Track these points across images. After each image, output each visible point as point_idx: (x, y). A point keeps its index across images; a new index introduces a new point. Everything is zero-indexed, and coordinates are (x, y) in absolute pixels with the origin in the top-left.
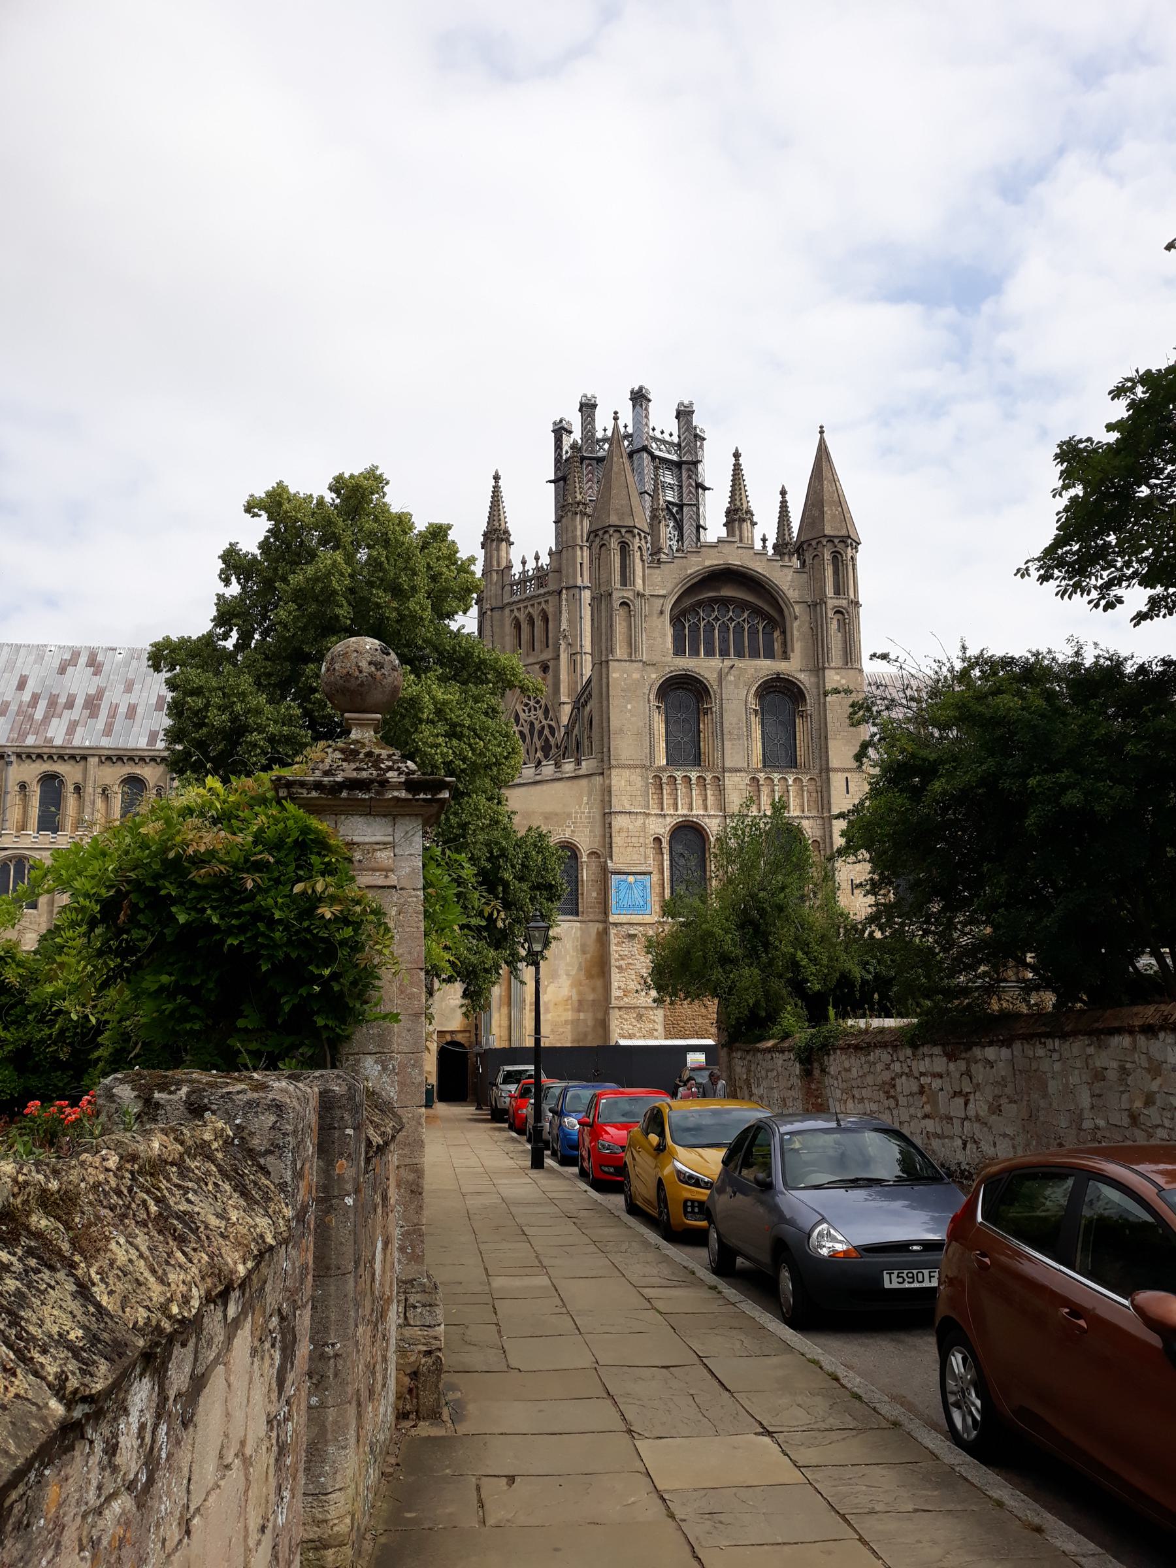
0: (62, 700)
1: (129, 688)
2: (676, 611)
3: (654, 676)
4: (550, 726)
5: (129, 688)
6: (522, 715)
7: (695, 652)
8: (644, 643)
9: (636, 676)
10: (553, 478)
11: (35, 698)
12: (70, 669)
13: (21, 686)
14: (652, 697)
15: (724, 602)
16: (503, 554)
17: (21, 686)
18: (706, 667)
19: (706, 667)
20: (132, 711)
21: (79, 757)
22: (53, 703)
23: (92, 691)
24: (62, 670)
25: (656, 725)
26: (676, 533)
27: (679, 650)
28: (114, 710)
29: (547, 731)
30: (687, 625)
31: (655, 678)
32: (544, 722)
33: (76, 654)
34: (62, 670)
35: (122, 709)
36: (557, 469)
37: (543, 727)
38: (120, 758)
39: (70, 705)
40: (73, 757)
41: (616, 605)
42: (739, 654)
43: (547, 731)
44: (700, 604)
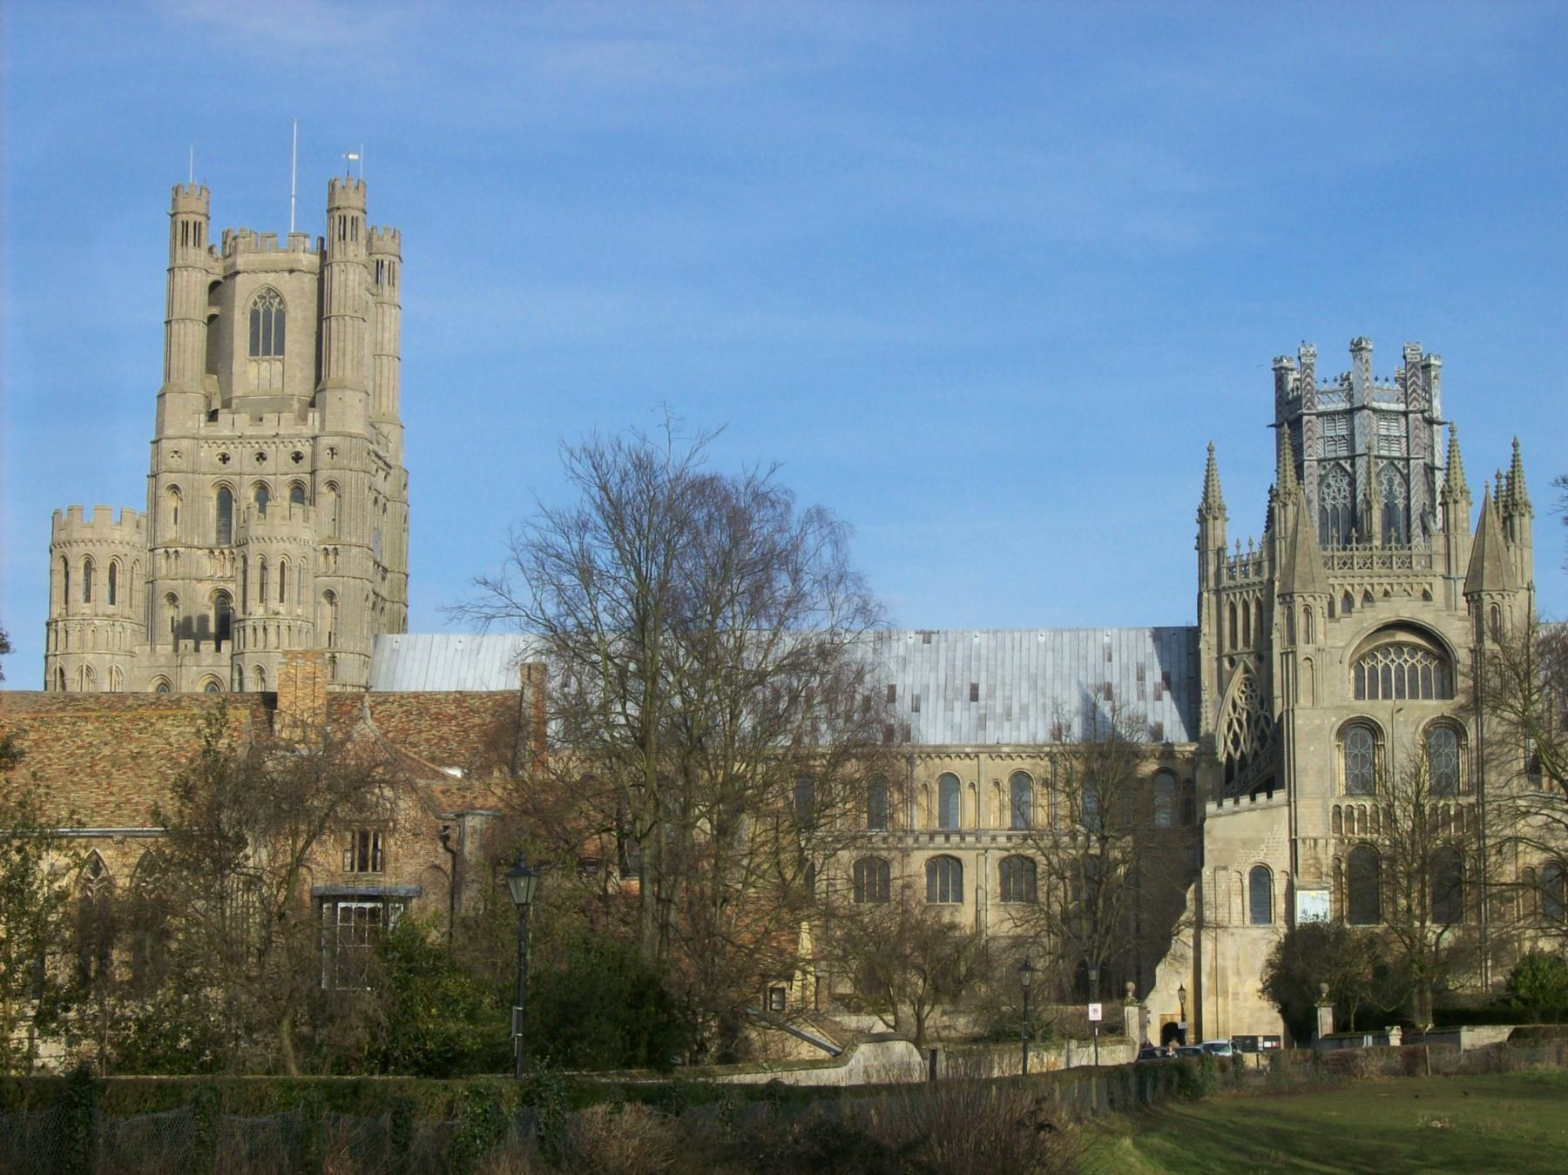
2: (1356, 657)
3: (1334, 719)
4: (1266, 717)
6: (1238, 701)
7: (1373, 696)
8: (1324, 690)
9: (1317, 722)
10: (1273, 421)
14: (1333, 737)
15: (1399, 646)
16: (1219, 532)
18: (1378, 710)
19: (1378, 710)
25: (1336, 761)
26: (1403, 490)
27: (1359, 694)
29: (1262, 722)
30: (1366, 667)
31: (1335, 721)
32: (1260, 712)
36: (1278, 412)
37: (1259, 717)
41: (1300, 659)
42: (1414, 695)
43: (1262, 722)
44: (1377, 648)
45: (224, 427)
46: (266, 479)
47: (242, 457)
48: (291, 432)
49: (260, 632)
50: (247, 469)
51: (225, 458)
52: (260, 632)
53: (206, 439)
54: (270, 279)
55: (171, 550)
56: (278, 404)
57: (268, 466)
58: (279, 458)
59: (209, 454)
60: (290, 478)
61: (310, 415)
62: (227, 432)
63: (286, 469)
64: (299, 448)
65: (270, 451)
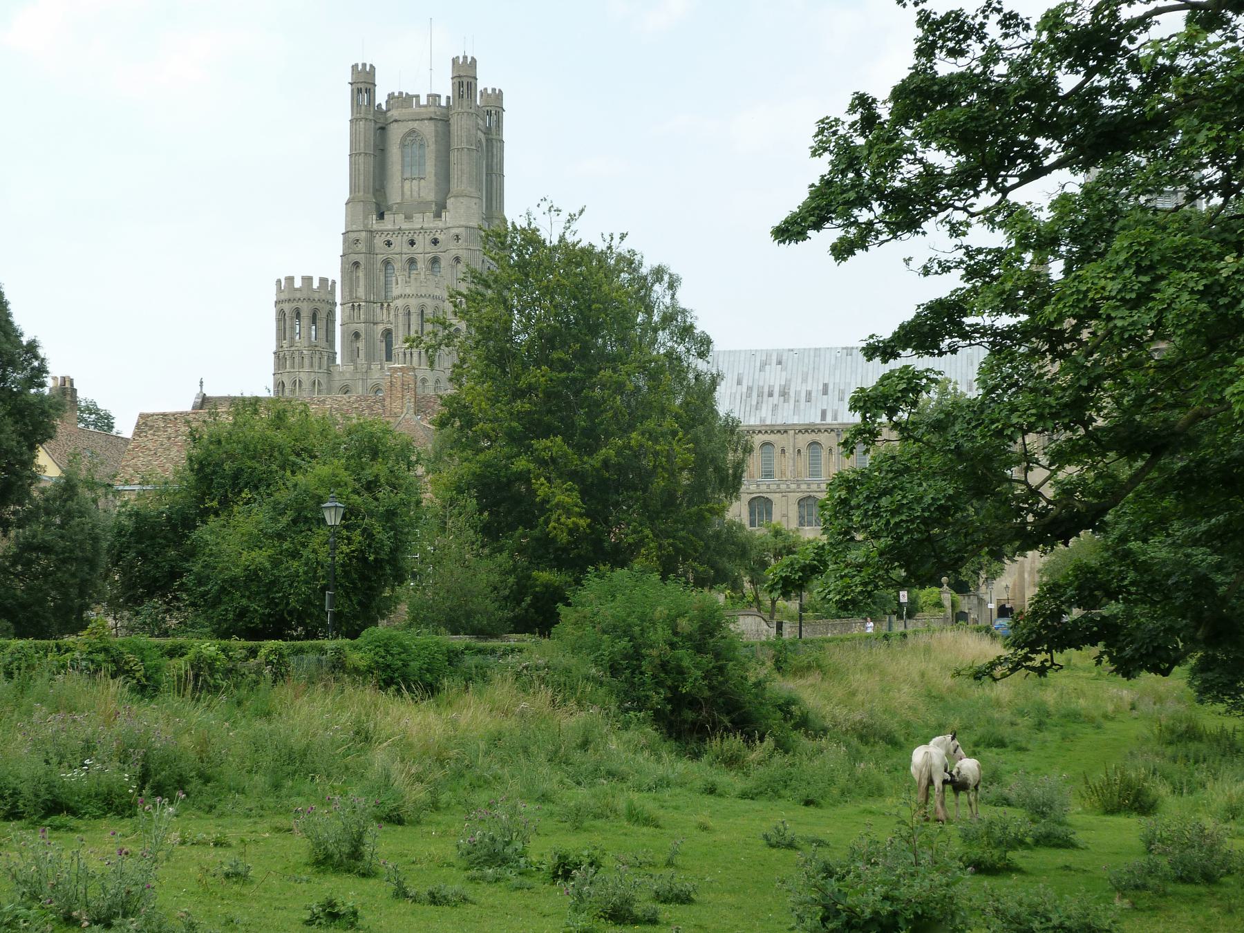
0: (766, 390)
1: (804, 380)
5: (804, 380)
11: (750, 389)
12: (767, 367)
13: (739, 383)
17: (739, 383)
20: (809, 394)
21: (783, 430)
22: (760, 395)
23: (783, 383)
24: (762, 368)
28: (797, 393)
33: (768, 354)
34: (762, 368)
35: (803, 395)
38: (806, 431)
39: (771, 395)
40: (779, 431)
45: (388, 224)
46: (415, 256)
47: (399, 243)
48: (431, 225)
49: (408, 356)
50: (405, 250)
51: (389, 244)
52: (408, 356)
53: (377, 231)
54: (416, 125)
55: (356, 304)
56: (422, 207)
57: (419, 247)
58: (423, 243)
59: (379, 241)
60: (431, 255)
61: (443, 214)
62: (390, 227)
63: (428, 250)
64: (437, 236)
65: (419, 240)
